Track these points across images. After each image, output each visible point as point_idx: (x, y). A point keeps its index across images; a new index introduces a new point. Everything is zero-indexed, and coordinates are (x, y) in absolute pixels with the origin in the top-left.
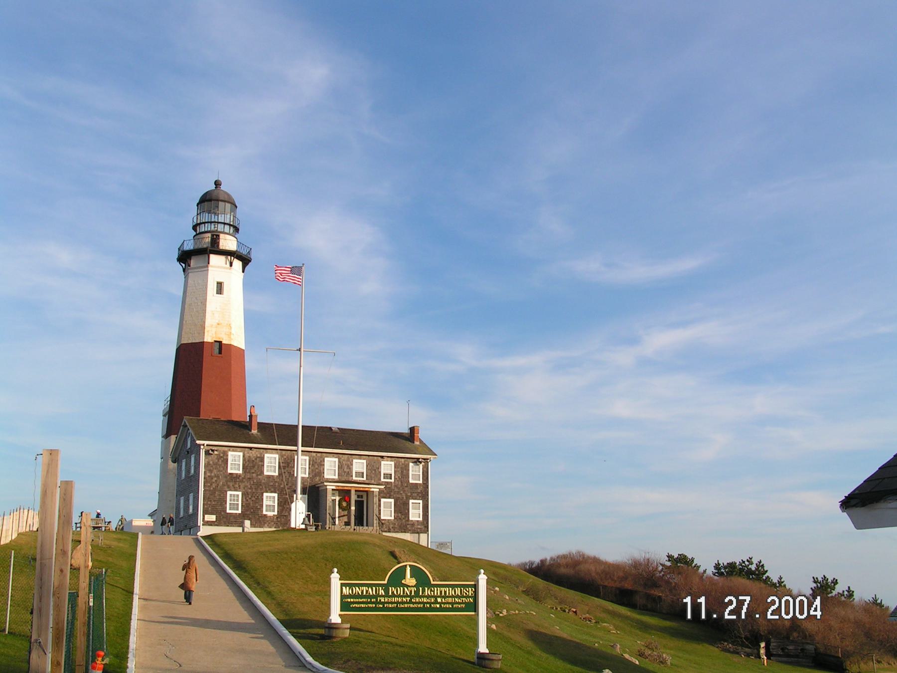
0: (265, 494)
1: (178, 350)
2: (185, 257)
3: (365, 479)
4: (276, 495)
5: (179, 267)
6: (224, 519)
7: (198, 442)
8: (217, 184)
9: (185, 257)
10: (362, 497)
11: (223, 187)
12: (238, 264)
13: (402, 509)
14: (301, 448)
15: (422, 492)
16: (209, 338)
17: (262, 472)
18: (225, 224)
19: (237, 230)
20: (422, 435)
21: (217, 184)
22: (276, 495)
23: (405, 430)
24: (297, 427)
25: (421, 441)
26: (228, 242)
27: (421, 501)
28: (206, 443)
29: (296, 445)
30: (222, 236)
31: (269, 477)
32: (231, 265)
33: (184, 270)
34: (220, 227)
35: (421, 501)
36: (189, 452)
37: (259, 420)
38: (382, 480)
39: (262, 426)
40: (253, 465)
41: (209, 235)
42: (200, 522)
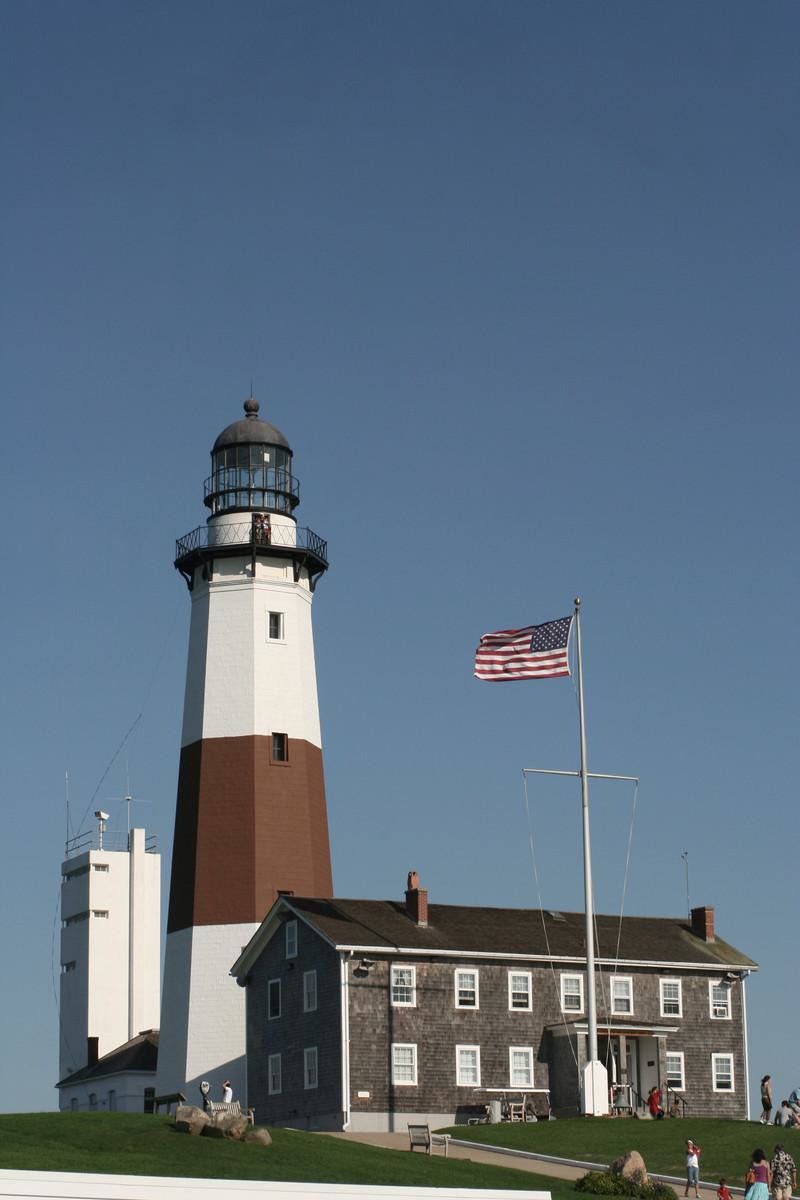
0: (459, 1048)
1: (183, 750)
3: (632, 1013)
4: (477, 1048)
5: (180, 581)
6: (390, 1100)
7: (339, 947)
14: (592, 961)
16: (263, 728)
18: (277, 493)
19: (294, 501)
20: (720, 927)
21: (250, 410)
22: (477, 1048)
23: (684, 915)
24: (583, 917)
25: (717, 938)
26: (283, 532)
28: (353, 948)
29: (585, 954)
31: (463, 1013)
33: (191, 586)
37: (431, 901)
38: (662, 1014)
39: (437, 913)
41: (247, 517)
42: (346, 1105)
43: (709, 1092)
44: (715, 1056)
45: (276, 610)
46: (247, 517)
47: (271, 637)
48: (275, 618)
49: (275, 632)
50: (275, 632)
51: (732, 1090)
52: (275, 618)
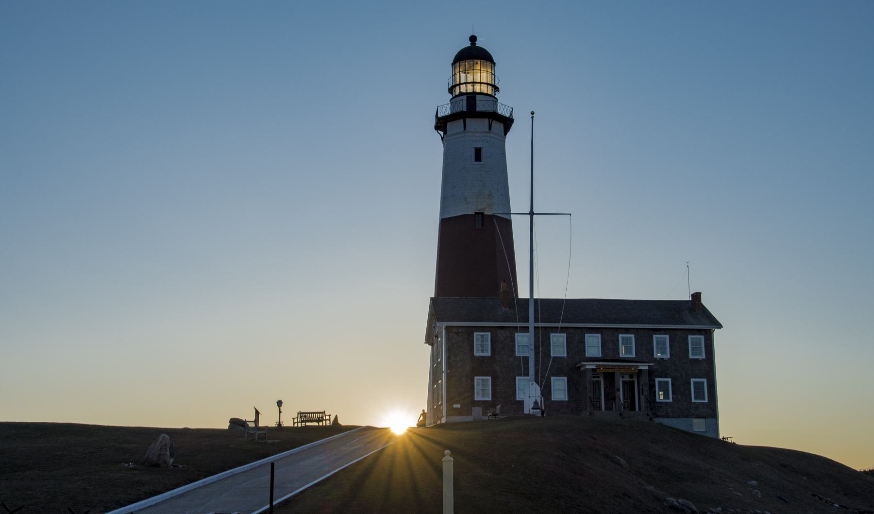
2: (442, 124)
5: (437, 136)
8: (473, 39)
9: (442, 124)
11: (478, 44)
12: (498, 127)
13: (681, 389)
15: (707, 368)
17: (513, 351)
20: (704, 301)
21: (473, 39)
23: (688, 298)
27: (705, 380)
29: (528, 321)
30: (478, 96)
32: (490, 128)
33: (442, 139)
34: (478, 88)
35: (705, 380)
36: (437, 336)
40: (503, 343)
41: (465, 97)
43: (691, 402)
44: (692, 380)
45: (479, 146)
46: (465, 97)
51: (706, 401)
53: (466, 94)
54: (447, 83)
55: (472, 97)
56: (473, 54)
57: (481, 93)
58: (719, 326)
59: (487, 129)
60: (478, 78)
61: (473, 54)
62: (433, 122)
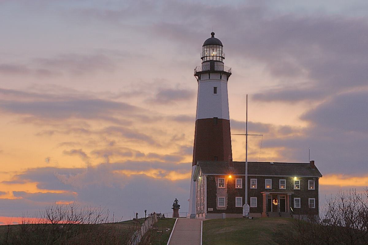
5: (195, 79)
8: (213, 34)
9: (197, 74)
10: (284, 197)
11: (215, 37)
21: (213, 34)
27: (314, 199)
33: (198, 80)
44: (309, 199)
46: (209, 63)
47: (214, 93)
48: (215, 89)
49: (215, 92)
50: (215, 92)
52: (215, 89)
53: (210, 61)
54: (199, 56)
55: (212, 62)
56: (213, 43)
57: (216, 61)
58: (321, 176)
59: (220, 79)
60: (214, 53)
61: (213, 43)
62: (194, 74)
